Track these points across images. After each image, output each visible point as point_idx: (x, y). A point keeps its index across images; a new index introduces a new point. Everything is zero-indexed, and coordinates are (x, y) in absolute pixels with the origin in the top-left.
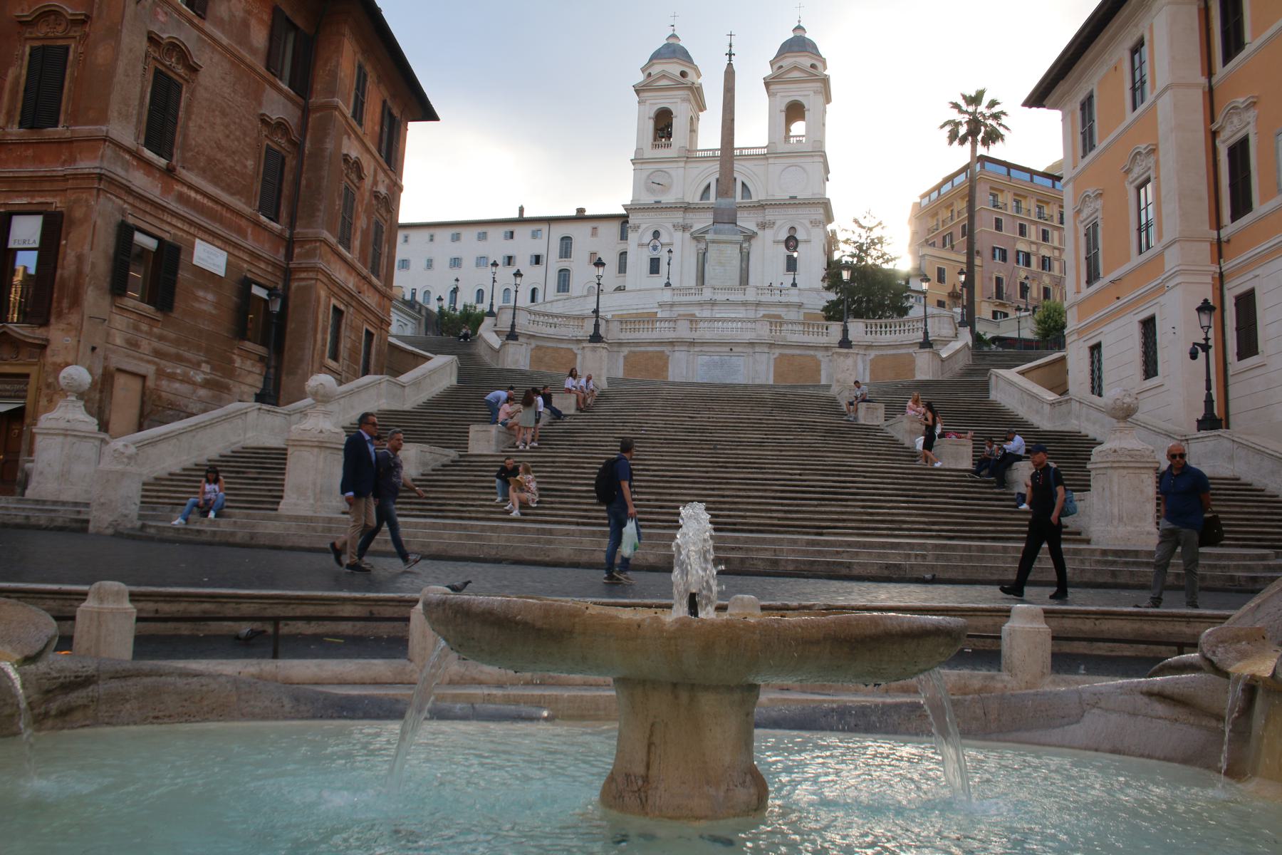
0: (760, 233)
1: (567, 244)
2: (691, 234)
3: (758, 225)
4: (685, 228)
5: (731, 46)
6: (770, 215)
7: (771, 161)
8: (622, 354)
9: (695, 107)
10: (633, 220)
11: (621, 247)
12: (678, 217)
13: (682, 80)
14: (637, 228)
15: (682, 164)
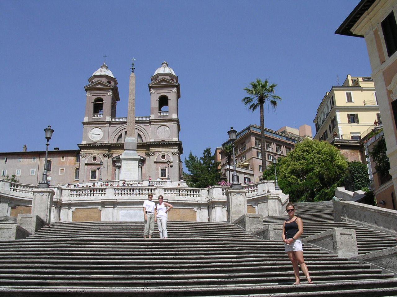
0: (147, 158)
1: (48, 164)
2: (113, 159)
3: (146, 154)
4: (110, 156)
5: (133, 65)
6: (152, 150)
7: (152, 123)
8: (71, 211)
9: (115, 99)
10: (82, 152)
11: (77, 166)
12: (106, 151)
13: (108, 85)
14: (84, 156)
15: (108, 125)
